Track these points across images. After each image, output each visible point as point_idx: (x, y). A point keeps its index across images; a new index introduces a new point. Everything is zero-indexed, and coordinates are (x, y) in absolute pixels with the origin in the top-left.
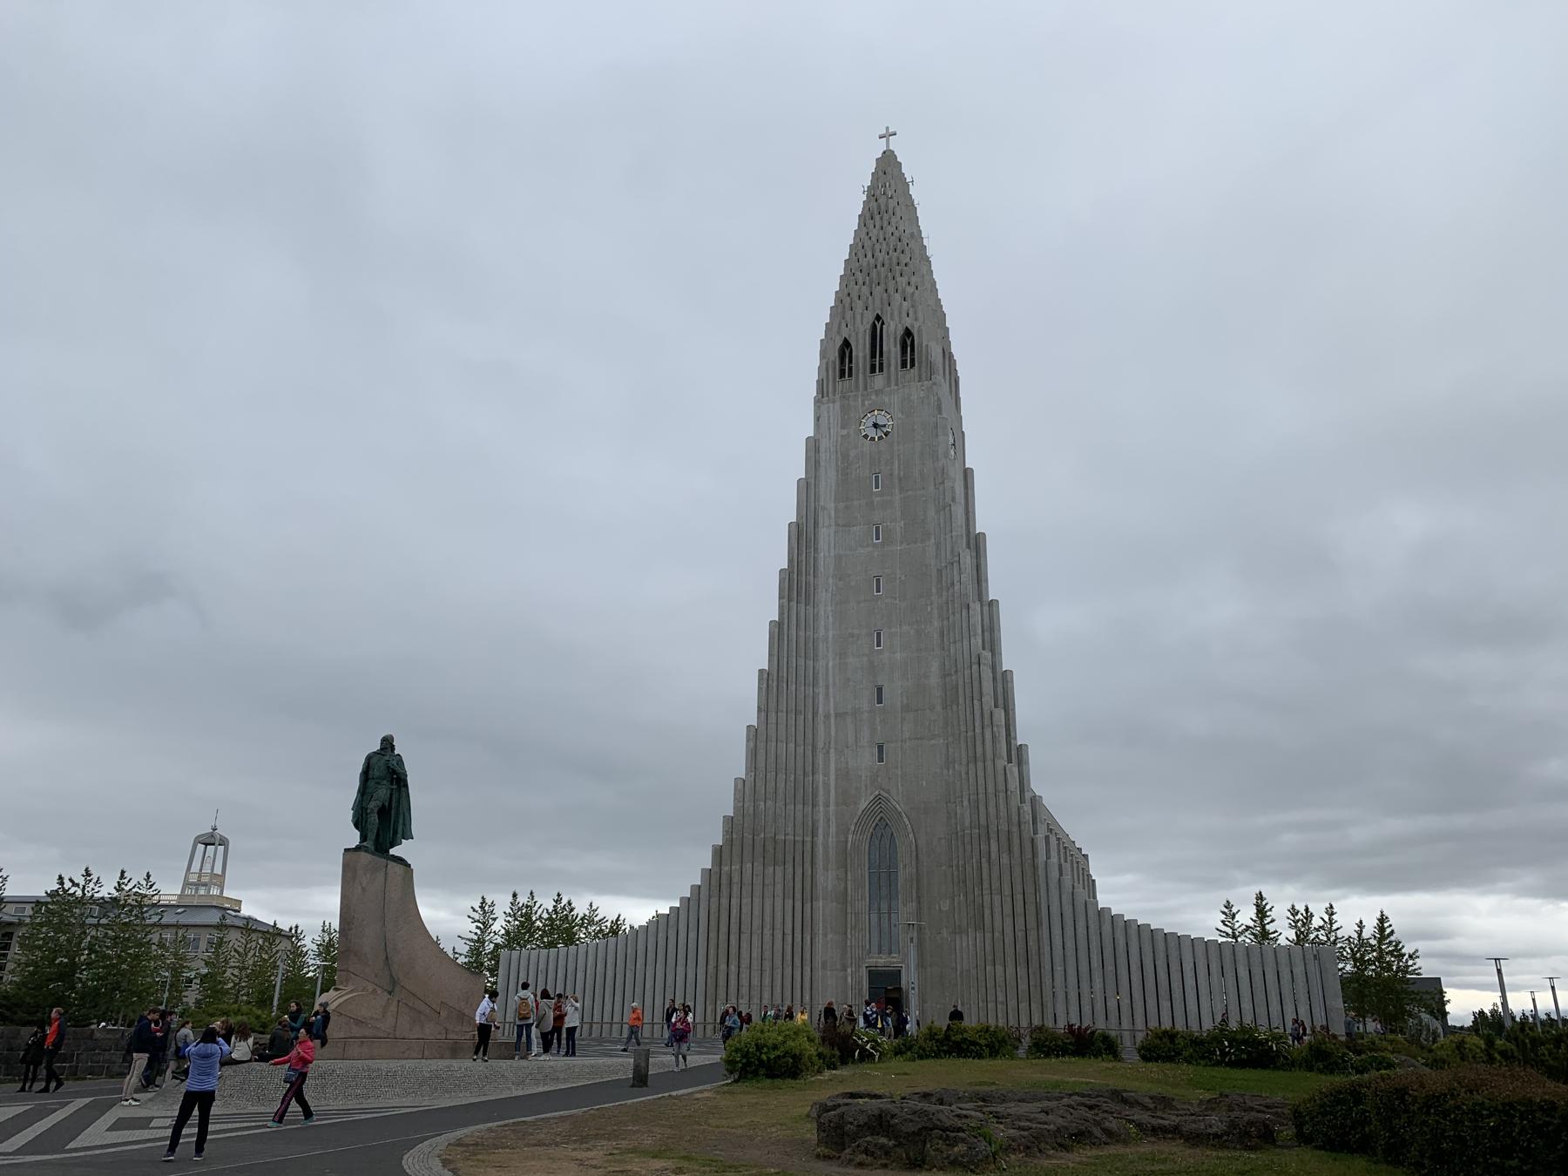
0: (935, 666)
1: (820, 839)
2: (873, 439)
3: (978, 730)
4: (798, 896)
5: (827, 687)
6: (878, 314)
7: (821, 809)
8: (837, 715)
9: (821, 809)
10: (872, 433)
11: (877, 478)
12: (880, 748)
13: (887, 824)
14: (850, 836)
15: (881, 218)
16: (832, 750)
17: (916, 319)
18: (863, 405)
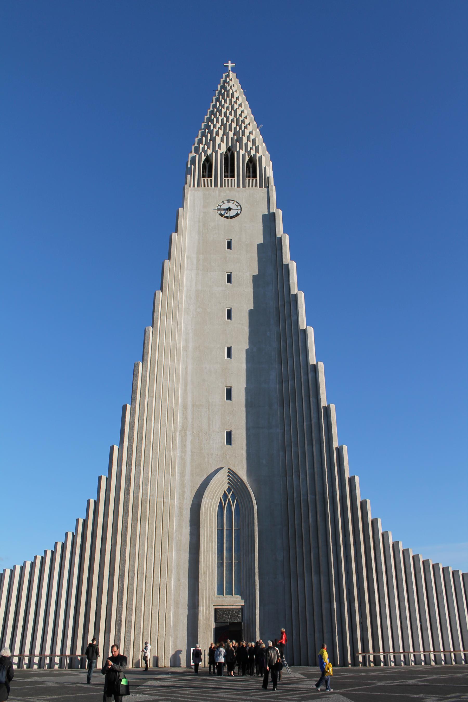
1: (176, 502)
2: (226, 217)
4: (158, 546)
5: (186, 385)
7: (177, 477)
8: (193, 406)
9: (177, 477)
15: (230, 101)
16: (189, 433)
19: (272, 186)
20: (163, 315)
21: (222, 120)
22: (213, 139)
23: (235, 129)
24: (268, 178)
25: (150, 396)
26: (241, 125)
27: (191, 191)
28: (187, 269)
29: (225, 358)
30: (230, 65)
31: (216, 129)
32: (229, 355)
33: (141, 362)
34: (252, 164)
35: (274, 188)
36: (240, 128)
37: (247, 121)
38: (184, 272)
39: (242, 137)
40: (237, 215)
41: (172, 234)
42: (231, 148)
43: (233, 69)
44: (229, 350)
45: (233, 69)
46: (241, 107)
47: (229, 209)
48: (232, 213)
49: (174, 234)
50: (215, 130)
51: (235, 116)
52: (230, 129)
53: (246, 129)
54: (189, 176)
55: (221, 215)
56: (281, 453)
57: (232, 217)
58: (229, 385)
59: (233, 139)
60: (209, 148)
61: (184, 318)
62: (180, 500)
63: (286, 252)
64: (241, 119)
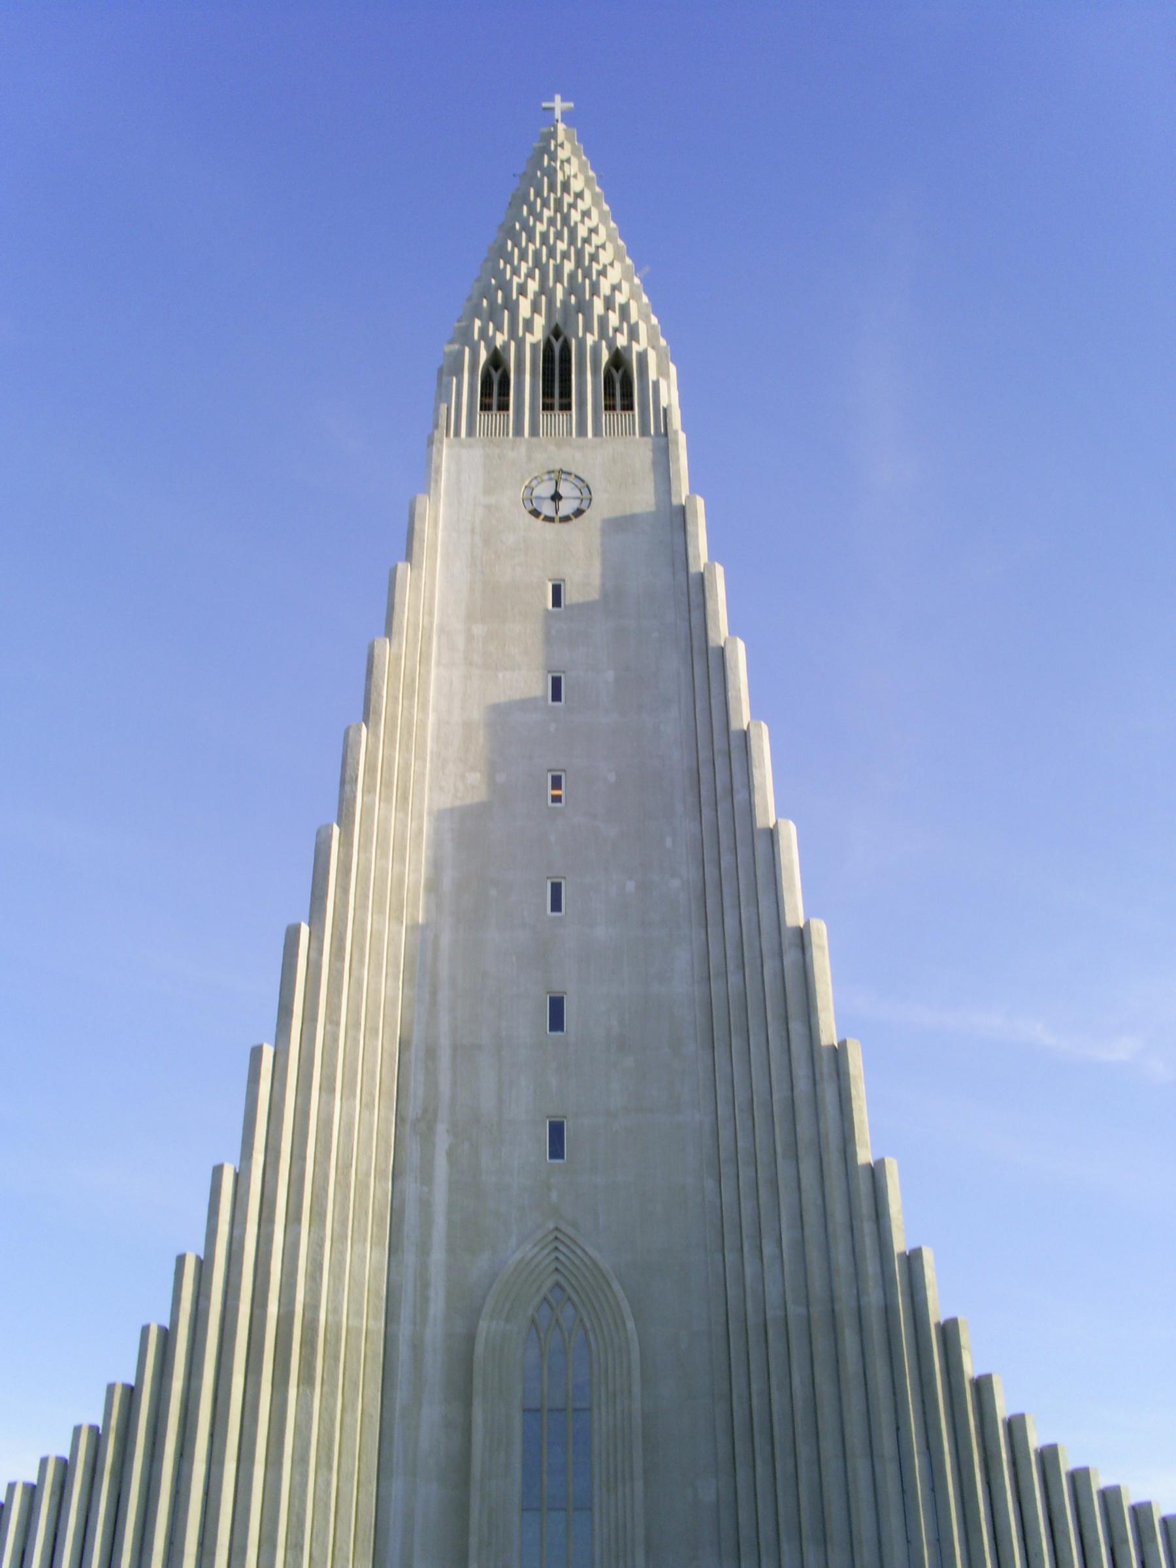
0: (683, 958)
3: (802, 1085)
6: (557, 326)
8: (455, 1048)
10: (547, 509)
11: (557, 591)
12: (557, 1130)
13: (569, 1299)
14: (483, 1325)
16: (442, 1128)
17: (633, 335)
18: (529, 458)
19: (676, 432)
20: (369, 792)
21: (537, 254)
22: (512, 306)
23: (572, 276)
24: (665, 410)
25: (333, 1020)
26: (590, 267)
27: (450, 447)
28: (439, 663)
29: (546, 910)
30: (559, 105)
31: (520, 277)
32: (556, 906)
33: (305, 922)
34: (621, 372)
35: (682, 438)
36: (587, 274)
37: (605, 257)
38: (429, 672)
39: (591, 300)
40: (579, 513)
41: (396, 565)
42: (560, 324)
43: (567, 117)
44: (556, 889)
45: (567, 117)
46: (590, 217)
47: (556, 497)
48: (566, 508)
49: (401, 566)
50: (516, 280)
51: (572, 240)
52: (558, 278)
53: (602, 278)
54: (443, 407)
55: (535, 513)
56: (710, 1184)
57: (565, 519)
58: (557, 988)
59: (565, 303)
60: (499, 328)
61: (431, 799)
62: (415, 1324)
63: (716, 612)
64: (589, 249)
